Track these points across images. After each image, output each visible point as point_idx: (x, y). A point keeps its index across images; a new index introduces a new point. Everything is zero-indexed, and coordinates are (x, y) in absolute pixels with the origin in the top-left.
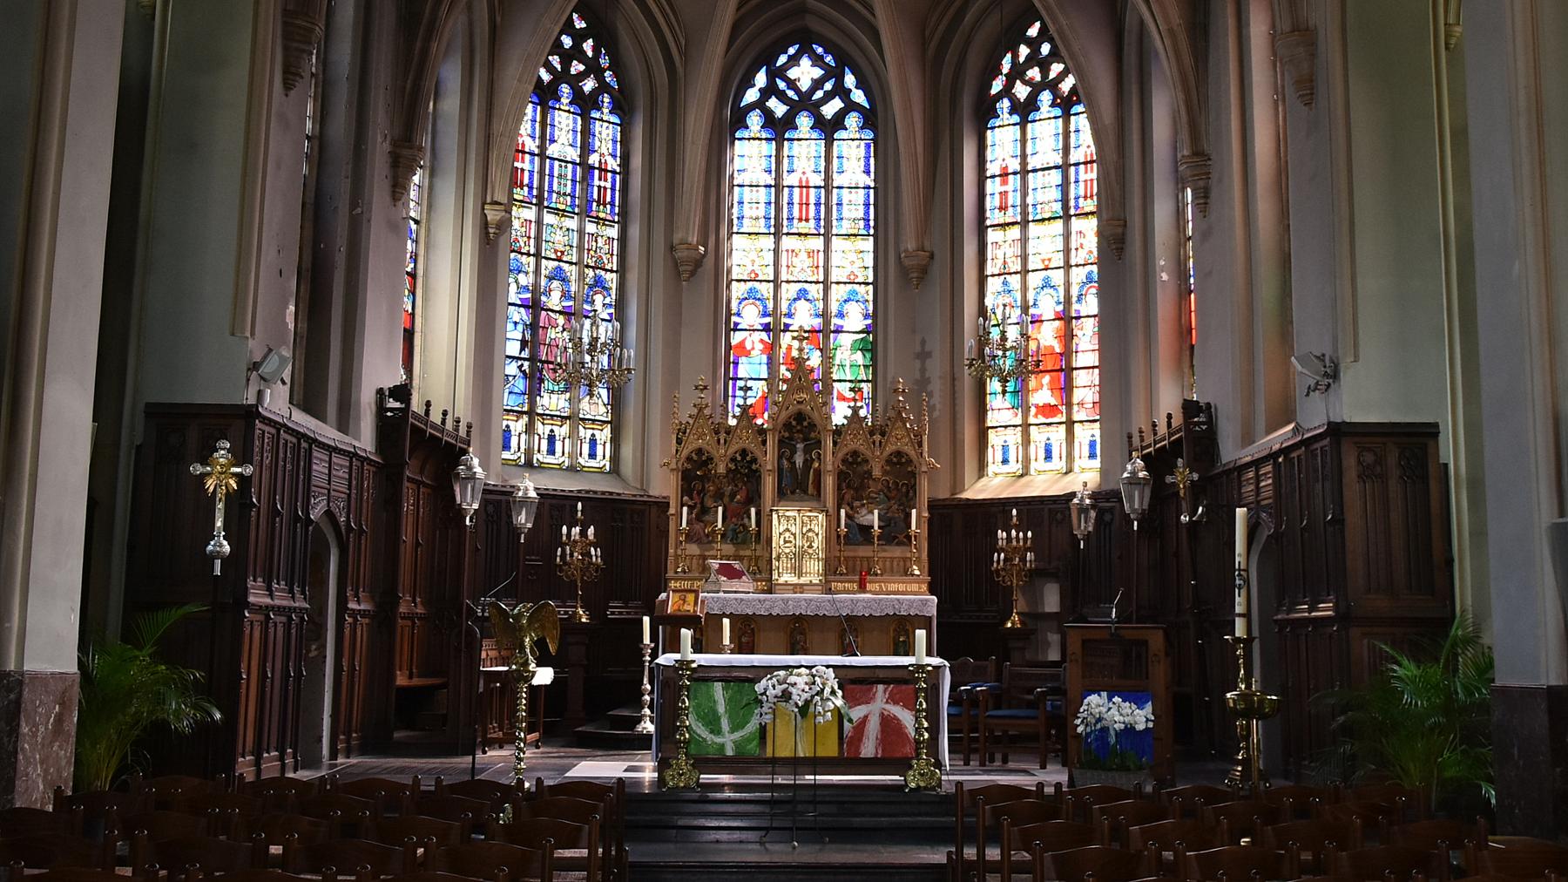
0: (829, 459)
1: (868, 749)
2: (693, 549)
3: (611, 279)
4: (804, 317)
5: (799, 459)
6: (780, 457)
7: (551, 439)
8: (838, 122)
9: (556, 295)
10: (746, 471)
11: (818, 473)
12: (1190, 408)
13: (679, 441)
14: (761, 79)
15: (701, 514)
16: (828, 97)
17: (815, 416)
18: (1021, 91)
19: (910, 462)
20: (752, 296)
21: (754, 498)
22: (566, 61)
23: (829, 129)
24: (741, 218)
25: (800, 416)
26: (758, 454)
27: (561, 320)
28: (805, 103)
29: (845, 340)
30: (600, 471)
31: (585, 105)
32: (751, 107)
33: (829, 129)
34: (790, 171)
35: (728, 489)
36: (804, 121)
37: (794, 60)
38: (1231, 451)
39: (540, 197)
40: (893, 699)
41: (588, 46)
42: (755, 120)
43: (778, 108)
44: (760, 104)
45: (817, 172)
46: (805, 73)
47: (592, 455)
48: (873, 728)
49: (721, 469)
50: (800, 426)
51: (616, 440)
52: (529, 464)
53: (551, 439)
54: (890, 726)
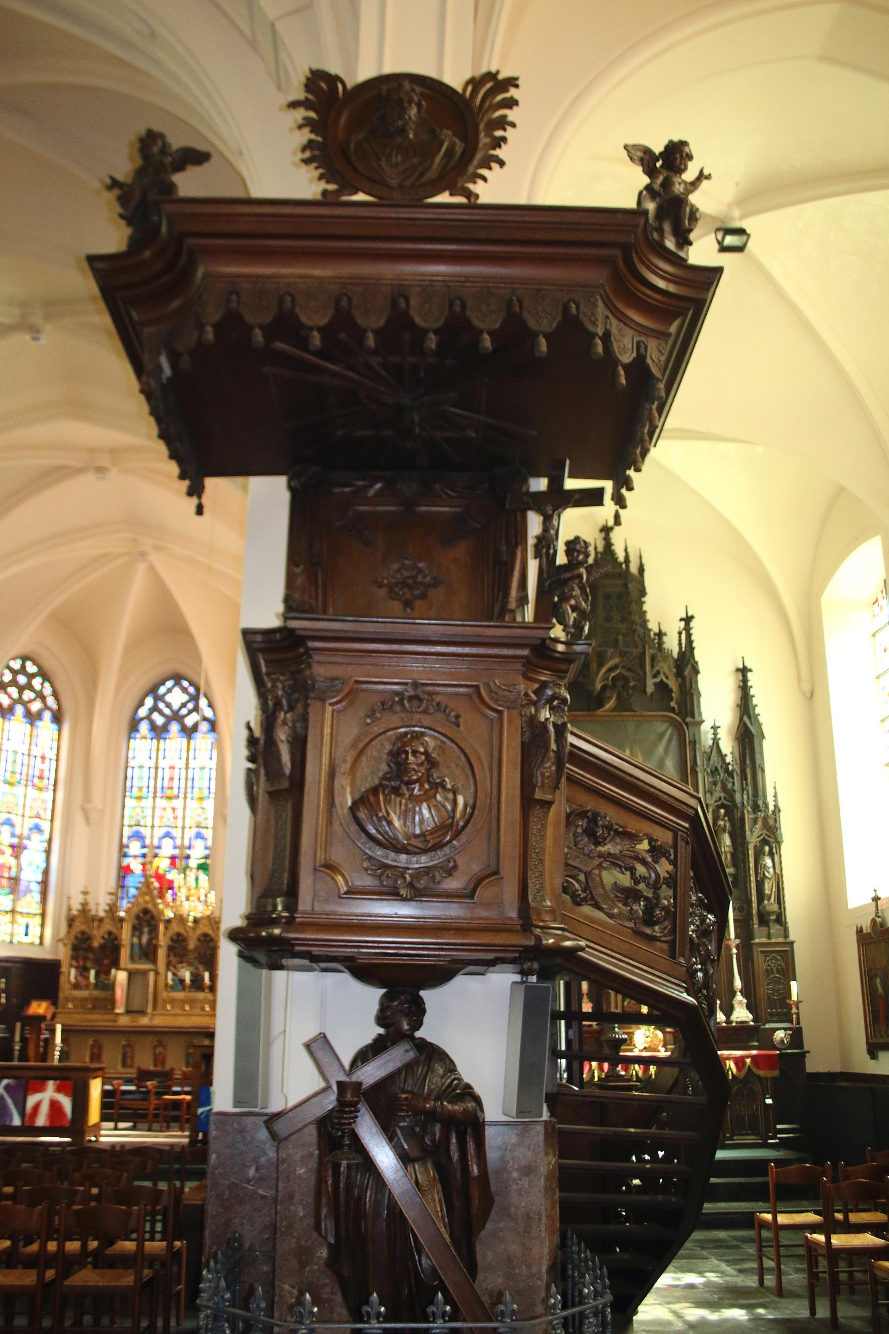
0: (163, 940)
1: (41, 1120)
3: (46, 825)
4: (167, 849)
5: (145, 939)
6: (133, 935)
13: (70, 926)
14: (149, 702)
15: (83, 971)
16: (190, 712)
19: (212, 940)
21: (116, 964)
22: (21, 689)
23: (189, 732)
25: (146, 911)
30: (32, 944)
33: (189, 732)
36: (174, 727)
40: (59, 1090)
42: (144, 727)
43: (159, 720)
44: (148, 717)
46: (177, 698)
48: (45, 1109)
50: (146, 919)
51: (43, 925)
54: (55, 1106)
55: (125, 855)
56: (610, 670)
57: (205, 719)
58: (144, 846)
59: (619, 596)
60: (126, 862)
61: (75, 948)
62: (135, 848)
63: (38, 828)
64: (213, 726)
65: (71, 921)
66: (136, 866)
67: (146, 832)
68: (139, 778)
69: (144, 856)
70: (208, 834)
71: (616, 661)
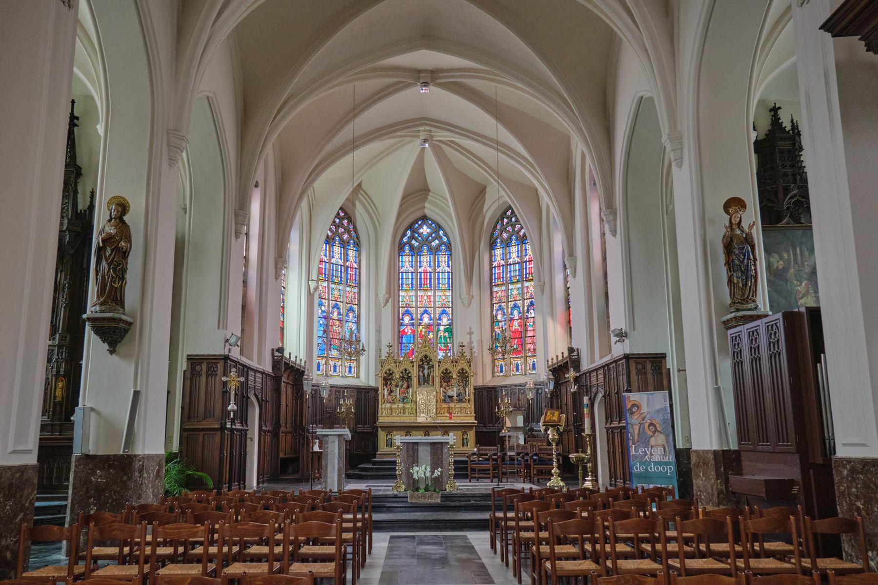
0: (437, 373)
2: (388, 405)
5: (426, 372)
7: (335, 367)
8: (438, 249)
9: (335, 314)
10: (406, 377)
11: (433, 377)
12: (571, 350)
14: (409, 233)
16: (434, 240)
17: (432, 356)
18: (505, 235)
20: (407, 313)
22: (337, 227)
24: (402, 284)
25: (426, 357)
26: (411, 370)
27: (338, 323)
28: (426, 241)
29: (442, 328)
30: (353, 377)
31: (344, 245)
32: (405, 244)
34: (420, 267)
35: (400, 384)
37: (421, 226)
38: (585, 366)
39: (329, 278)
41: (345, 222)
43: (416, 244)
44: (409, 243)
45: (430, 267)
46: (425, 230)
47: (350, 372)
49: (398, 376)
50: (426, 361)
52: (327, 375)
53: (335, 367)
55: (402, 325)
56: (792, 198)
57: (444, 243)
58: (412, 319)
59: (789, 151)
60: (402, 328)
61: (385, 379)
62: (407, 320)
63: (351, 310)
64: (449, 246)
65: (382, 363)
66: (408, 330)
67: (413, 310)
68: (407, 279)
69: (413, 324)
70: (449, 310)
71: (796, 191)
